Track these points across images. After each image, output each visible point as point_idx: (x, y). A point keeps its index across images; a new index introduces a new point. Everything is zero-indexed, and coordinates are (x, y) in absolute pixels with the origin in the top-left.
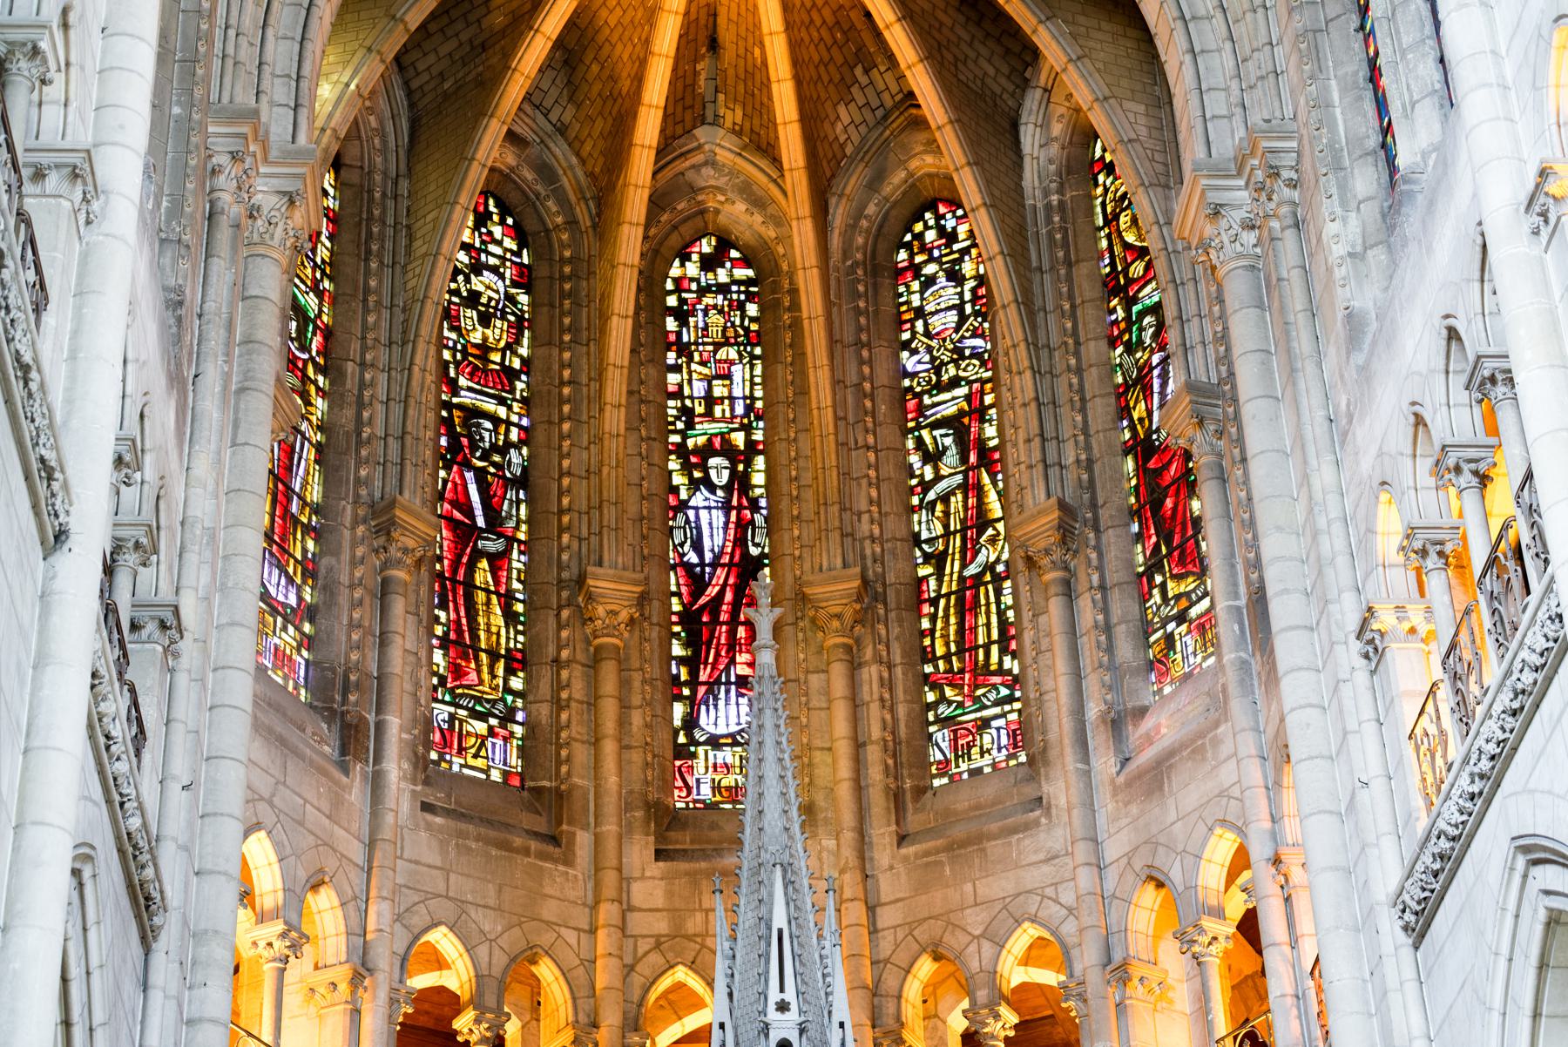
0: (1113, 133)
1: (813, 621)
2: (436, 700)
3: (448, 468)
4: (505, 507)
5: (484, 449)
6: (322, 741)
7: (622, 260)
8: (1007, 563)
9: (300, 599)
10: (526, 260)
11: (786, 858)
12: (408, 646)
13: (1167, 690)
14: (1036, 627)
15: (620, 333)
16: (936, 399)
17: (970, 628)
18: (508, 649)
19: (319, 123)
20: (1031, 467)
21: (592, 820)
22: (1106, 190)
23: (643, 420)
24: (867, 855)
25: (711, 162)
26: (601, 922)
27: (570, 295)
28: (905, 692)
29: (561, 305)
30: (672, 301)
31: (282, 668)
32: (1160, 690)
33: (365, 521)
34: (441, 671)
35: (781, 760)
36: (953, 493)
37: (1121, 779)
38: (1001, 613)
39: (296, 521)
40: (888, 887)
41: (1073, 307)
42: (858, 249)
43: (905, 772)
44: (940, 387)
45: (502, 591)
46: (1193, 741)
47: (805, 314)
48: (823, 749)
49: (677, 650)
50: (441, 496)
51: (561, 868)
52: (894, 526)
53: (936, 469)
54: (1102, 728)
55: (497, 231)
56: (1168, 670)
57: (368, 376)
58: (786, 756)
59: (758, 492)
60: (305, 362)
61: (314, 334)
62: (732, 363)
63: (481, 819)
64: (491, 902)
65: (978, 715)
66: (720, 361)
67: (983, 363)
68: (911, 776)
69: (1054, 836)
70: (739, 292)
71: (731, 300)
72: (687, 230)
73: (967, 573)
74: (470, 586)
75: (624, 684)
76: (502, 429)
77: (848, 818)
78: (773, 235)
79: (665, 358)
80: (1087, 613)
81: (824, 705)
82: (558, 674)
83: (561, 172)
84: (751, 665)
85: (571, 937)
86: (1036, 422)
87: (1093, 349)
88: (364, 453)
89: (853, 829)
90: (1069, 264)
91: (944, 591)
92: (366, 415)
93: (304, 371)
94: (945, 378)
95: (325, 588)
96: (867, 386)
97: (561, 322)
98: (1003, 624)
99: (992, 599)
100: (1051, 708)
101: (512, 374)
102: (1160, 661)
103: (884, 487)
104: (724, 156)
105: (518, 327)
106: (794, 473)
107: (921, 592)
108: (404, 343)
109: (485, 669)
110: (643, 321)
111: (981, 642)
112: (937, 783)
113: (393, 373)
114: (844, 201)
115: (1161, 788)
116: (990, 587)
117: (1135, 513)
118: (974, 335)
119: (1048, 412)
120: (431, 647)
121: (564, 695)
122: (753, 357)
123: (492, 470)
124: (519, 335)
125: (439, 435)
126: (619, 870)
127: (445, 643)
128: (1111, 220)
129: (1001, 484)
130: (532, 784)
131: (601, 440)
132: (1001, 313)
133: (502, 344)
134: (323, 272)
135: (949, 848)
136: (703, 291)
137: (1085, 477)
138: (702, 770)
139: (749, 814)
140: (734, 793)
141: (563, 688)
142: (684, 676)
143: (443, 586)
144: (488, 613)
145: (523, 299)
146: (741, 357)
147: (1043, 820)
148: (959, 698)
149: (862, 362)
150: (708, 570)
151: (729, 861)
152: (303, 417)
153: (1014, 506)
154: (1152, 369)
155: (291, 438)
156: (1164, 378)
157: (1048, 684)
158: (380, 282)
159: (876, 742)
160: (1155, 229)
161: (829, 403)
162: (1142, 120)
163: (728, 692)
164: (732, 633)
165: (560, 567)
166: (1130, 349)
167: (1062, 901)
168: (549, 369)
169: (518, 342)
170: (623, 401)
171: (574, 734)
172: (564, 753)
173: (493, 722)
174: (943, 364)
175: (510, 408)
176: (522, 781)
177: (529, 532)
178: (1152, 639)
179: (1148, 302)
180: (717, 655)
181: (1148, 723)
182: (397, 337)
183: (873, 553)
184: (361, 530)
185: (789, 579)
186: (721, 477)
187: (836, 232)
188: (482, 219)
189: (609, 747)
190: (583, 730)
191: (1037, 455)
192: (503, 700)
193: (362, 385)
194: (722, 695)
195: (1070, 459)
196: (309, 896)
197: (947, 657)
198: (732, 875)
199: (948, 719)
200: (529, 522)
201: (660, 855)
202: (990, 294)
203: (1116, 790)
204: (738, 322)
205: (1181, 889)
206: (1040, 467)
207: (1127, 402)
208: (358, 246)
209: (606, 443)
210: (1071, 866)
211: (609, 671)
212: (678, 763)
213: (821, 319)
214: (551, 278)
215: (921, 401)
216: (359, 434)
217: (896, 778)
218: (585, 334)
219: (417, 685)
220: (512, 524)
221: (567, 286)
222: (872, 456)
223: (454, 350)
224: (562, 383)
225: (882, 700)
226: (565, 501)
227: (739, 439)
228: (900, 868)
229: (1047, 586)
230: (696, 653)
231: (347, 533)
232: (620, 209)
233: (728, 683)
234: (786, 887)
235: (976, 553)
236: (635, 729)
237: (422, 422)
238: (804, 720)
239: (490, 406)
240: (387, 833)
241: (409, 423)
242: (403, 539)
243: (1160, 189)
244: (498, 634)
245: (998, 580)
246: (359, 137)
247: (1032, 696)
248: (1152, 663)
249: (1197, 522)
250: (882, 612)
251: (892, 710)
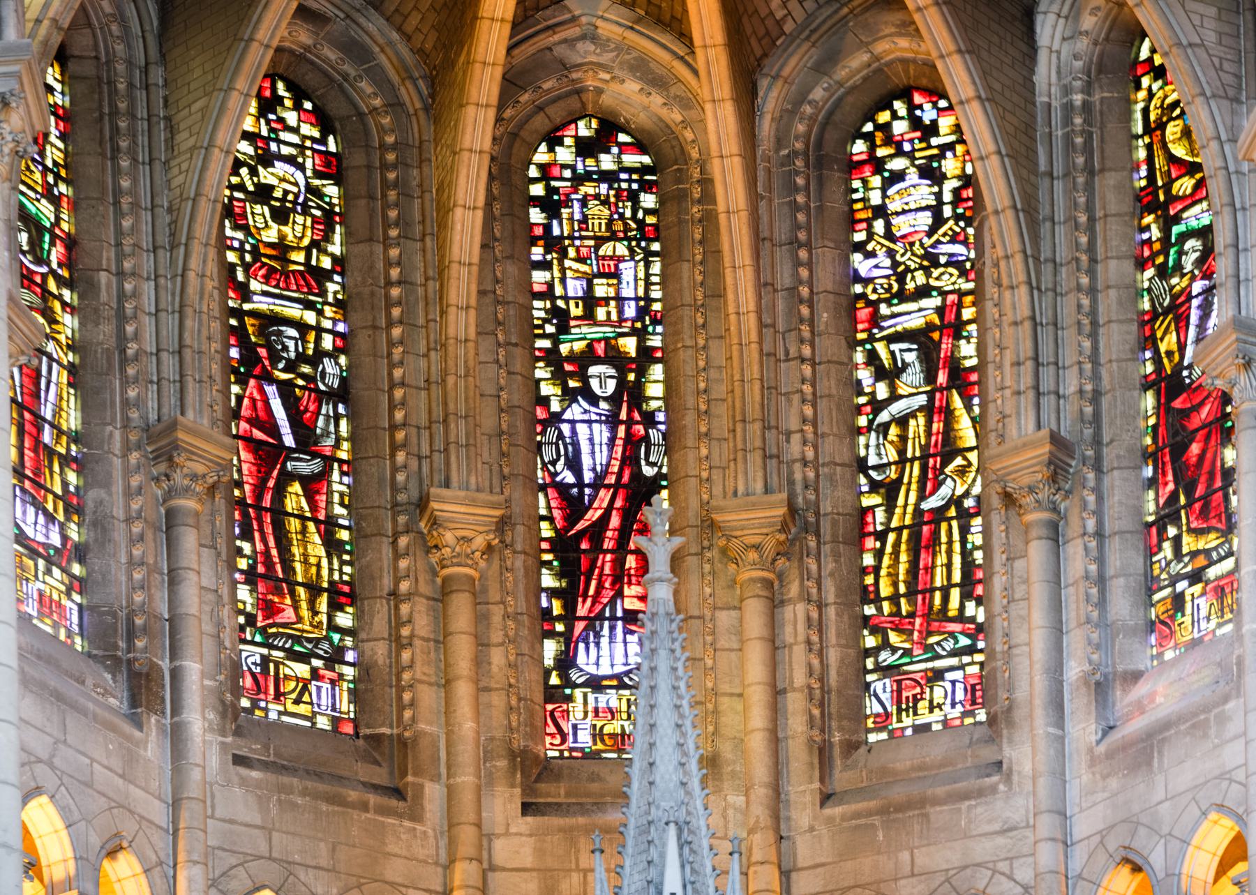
0: (1167, 33)
1: (724, 551)
2: (244, 641)
3: (243, 382)
4: (321, 422)
5: (288, 360)
6: (106, 693)
7: (467, 144)
8: (978, 498)
9: (65, 538)
10: (332, 148)
11: (682, 815)
12: (205, 583)
13: (1169, 655)
14: (1010, 573)
16: (896, 309)
17: (926, 568)
18: (331, 582)
19: (32, 14)
20: (1018, 393)
21: (443, 771)
22: (1151, 95)
23: (500, 324)
24: (782, 814)
25: (591, 36)
26: (457, 883)
27: (396, 185)
28: (838, 635)
29: (384, 196)
30: (537, 190)
31: (50, 616)
32: (1160, 655)
33: (139, 447)
34: (249, 608)
35: (677, 707)
36: (913, 415)
37: (1102, 749)
38: (965, 554)
39: (51, 452)
40: (805, 850)
41: (1092, 220)
42: (797, 138)
43: (834, 724)
44: (902, 296)
45: (322, 516)
46: (1195, 714)
47: (721, 207)
48: (732, 695)
49: (548, 580)
50: (236, 414)
51: (407, 823)
52: (833, 448)
53: (893, 388)
54: (1083, 690)
55: (291, 118)
56: (1172, 633)
57: (128, 287)
58: (685, 703)
59: (654, 405)
60: (44, 277)
61: (52, 244)
62: (621, 259)
63: (307, 772)
64: (323, 862)
65: (930, 665)
66: (604, 258)
67: (964, 273)
68: (841, 729)
70: (630, 181)
71: (619, 190)
72: (557, 113)
73: (925, 506)
74: (279, 514)
75: (481, 618)
76: (312, 337)
77: (760, 770)
78: (679, 118)
79: (529, 253)
80: (1076, 560)
81: (736, 646)
82: (397, 608)
83: (377, 49)
84: (643, 598)
86: (1029, 344)
87: (1115, 269)
88: (131, 371)
89: (767, 786)
90: (1090, 172)
91: (895, 523)
92: (130, 329)
93: (43, 286)
94: (910, 286)
95: (95, 524)
96: (805, 291)
97: (385, 216)
98: (968, 566)
99: (956, 536)
100: (1021, 664)
101: (321, 276)
102: (1163, 623)
103: (822, 405)
104: (606, 30)
105: (328, 220)
106: (702, 385)
107: (864, 523)
108: (173, 247)
109: (304, 605)
110: (497, 212)
111: (938, 583)
112: (872, 738)
113: (162, 281)
114: (780, 83)
115: (1149, 763)
116: (954, 524)
117: (1152, 456)
118: (954, 240)
119: (1046, 336)
120: (234, 583)
121: (405, 632)
122: (649, 254)
123: (300, 382)
124: (329, 230)
125: (228, 346)
126: (479, 826)
127: (251, 577)
128: (1154, 129)
129: (977, 410)
130: (368, 731)
131: (444, 346)
132: (992, 221)
133: (306, 242)
134: (57, 176)
135: (883, 811)
136: (579, 180)
137: (1089, 410)
138: (580, 715)
139: (637, 765)
140: (621, 741)
141: (404, 624)
142: (557, 608)
143: (245, 515)
144: (304, 542)
145: (332, 190)
146: (632, 252)
147: (1002, 787)
148: (907, 645)
149: (798, 263)
150: (587, 491)
151: (612, 817)
152: (47, 337)
153: (992, 436)
154: (1190, 298)
155: (35, 362)
157: (1020, 636)
158: (135, 181)
159: (800, 690)
160: (1214, 145)
161: (752, 306)
162: (1210, 24)
163: (612, 628)
164: (619, 563)
165: (395, 488)
166: (1163, 272)
167: (1018, 878)
168: (371, 267)
169: (328, 238)
170: (473, 302)
171: (419, 676)
172: (407, 696)
173: (317, 663)
174: (908, 270)
175: (320, 313)
176: (356, 727)
177: (353, 450)
178: (1156, 597)
179: (1194, 224)
180: (600, 587)
181: (1141, 690)
182: (163, 239)
183: (805, 479)
184: (134, 457)
185: (694, 503)
187: (768, 118)
188: (268, 105)
189: (463, 690)
190: (431, 671)
191: (1027, 380)
192: (327, 638)
193: (122, 296)
194: (606, 631)
196: (106, 864)
197: (894, 599)
198: (616, 832)
199: (889, 667)
200: (352, 438)
201: (527, 808)
202: (978, 196)
203: (1093, 761)
204: (628, 214)
205: (1161, 875)
206: (1031, 394)
207: (1153, 332)
208: (101, 143)
209: (451, 349)
210: (1032, 840)
211: (461, 611)
212: (550, 707)
213: (744, 215)
214: (369, 167)
215: (876, 310)
216: (123, 351)
217: (822, 731)
218: (418, 229)
219: (219, 625)
220: (330, 441)
221: (392, 176)
222: (807, 370)
223: (241, 250)
224: (389, 283)
225: (809, 642)
226: (399, 416)
227: (629, 345)
228: (823, 830)
229: (1028, 527)
230: (573, 585)
231: (117, 462)
232: (462, 90)
233: (613, 618)
234: (681, 847)
235: (938, 485)
236: (495, 669)
237: (205, 333)
238: (709, 662)
239: (293, 311)
240: (193, 789)
241: (187, 335)
242: (189, 464)
243: (1226, 103)
244: (319, 566)
245: (965, 517)
246: (90, 25)
247: (998, 648)
248: (1152, 623)
249: (1229, 475)
250: (812, 544)
251: (821, 654)
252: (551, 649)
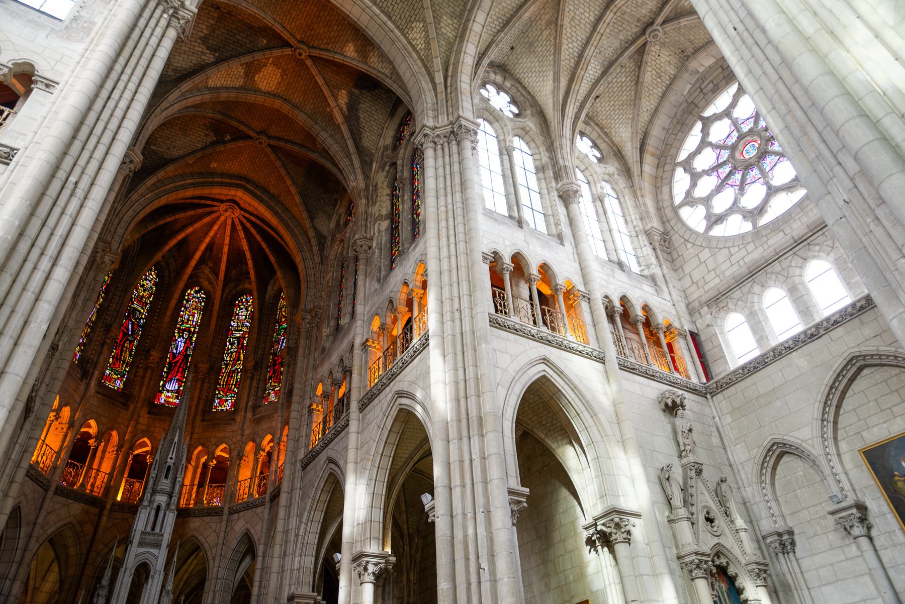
15: (173, 302)
38: (237, 379)
40: (196, 430)
49: (165, 370)
69: (235, 427)
80: (254, 384)
85: (122, 427)
127: (113, 357)
144: (126, 352)
156: (283, 342)
166: (277, 335)
181: (261, 409)
186: (186, 336)
193: (112, 298)
195: (259, 353)
197: (223, 385)
201: (149, 413)
227: (192, 329)
245: (238, 373)
252: (162, 383)
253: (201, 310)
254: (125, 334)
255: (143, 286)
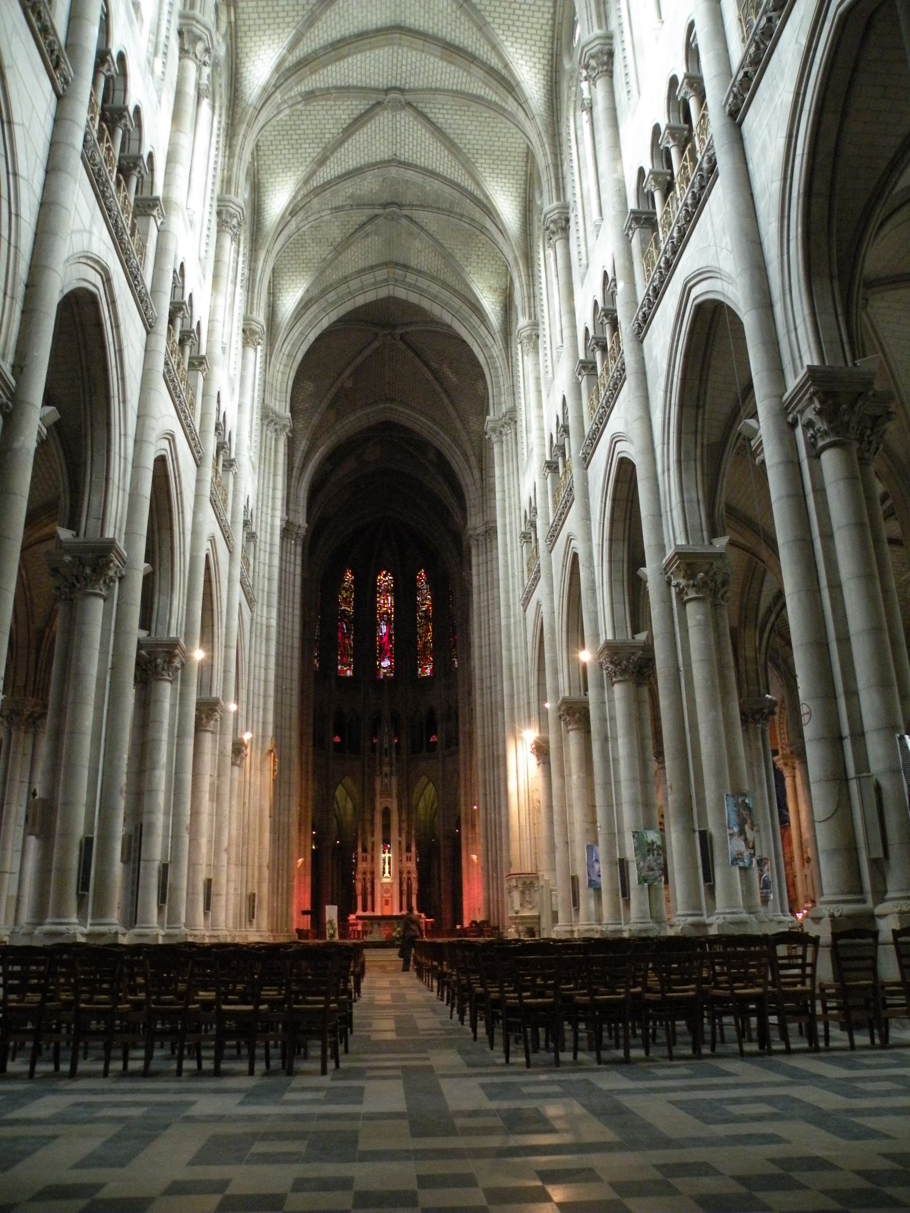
253: (392, 591)
254: (343, 634)
255: (344, 588)
